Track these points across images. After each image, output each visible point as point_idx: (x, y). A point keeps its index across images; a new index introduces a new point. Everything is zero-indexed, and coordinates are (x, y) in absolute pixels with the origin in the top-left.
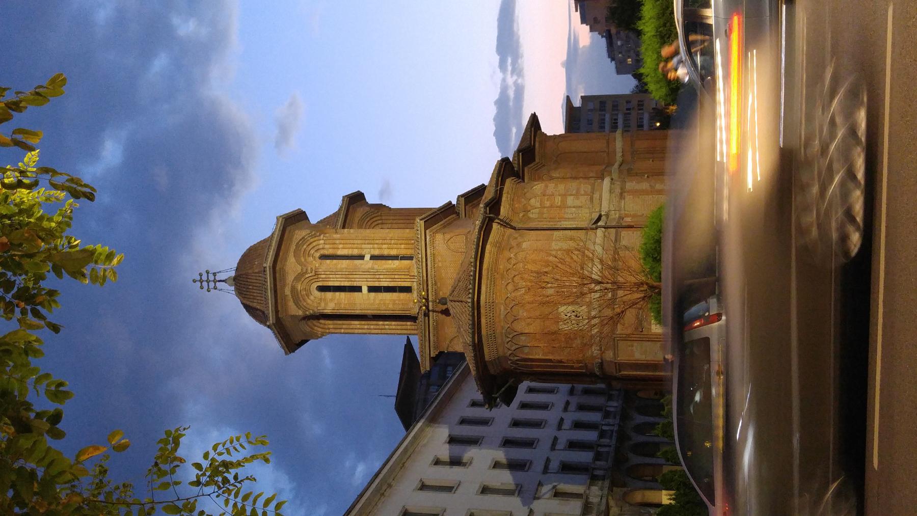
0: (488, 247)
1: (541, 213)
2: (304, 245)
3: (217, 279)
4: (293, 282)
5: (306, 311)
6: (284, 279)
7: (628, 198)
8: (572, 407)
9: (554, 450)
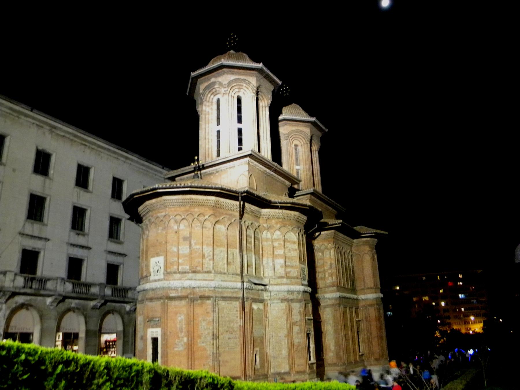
0: (213, 198)
1: (267, 240)
5: (203, 95)
6: (219, 75)
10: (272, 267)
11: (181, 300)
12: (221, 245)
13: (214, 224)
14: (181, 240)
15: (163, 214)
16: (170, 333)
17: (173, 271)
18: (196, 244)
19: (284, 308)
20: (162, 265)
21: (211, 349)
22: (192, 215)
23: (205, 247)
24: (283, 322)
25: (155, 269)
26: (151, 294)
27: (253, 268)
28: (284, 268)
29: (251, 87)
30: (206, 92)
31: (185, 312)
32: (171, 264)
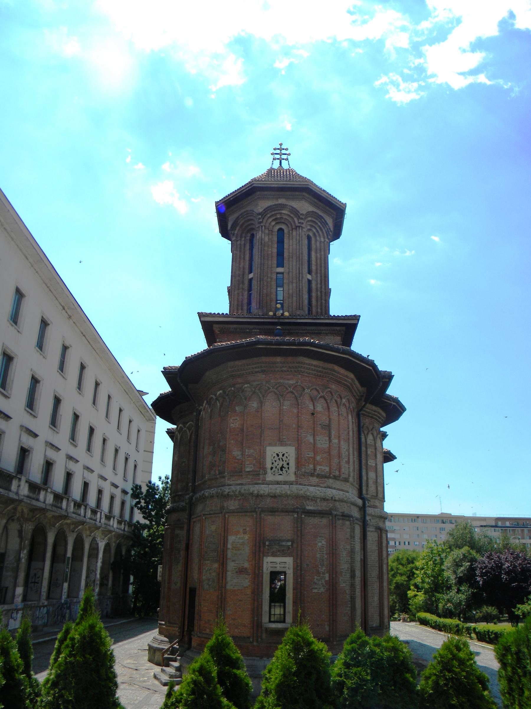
2: (321, 223)
3: (283, 161)
4: (291, 206)
5: (262, 216)
6: (293, 199)
8: (114, 490)
9: (84, 469)
11: (322, 517)
14: (319, 428)
16: (308, 565)
22: (331, 393)
23: (342, 443)
25: (276, 464)
29: (326, 229)
30: (268, 214)
32: (306, 460)
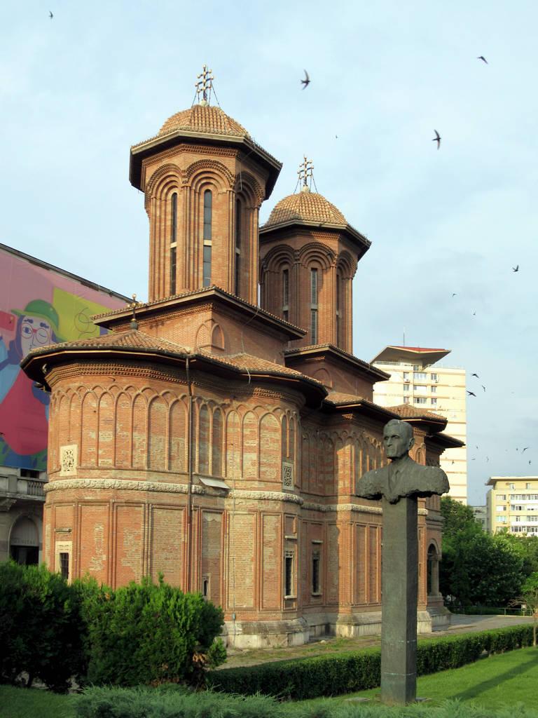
1: (234, 425)
7: (252, 519)
10: (239, 465)
12: (162, 433)
13: (150, 400)
15: (77, 384)
17: (89, 465)
18: (122, 429)
19: (253, 521)
20: (75, 457)
21: (141, 572)
24: (251, 541)
26: (59, 496)
27: (208, 464)
28: (257, 465)
31: (106, 521)
